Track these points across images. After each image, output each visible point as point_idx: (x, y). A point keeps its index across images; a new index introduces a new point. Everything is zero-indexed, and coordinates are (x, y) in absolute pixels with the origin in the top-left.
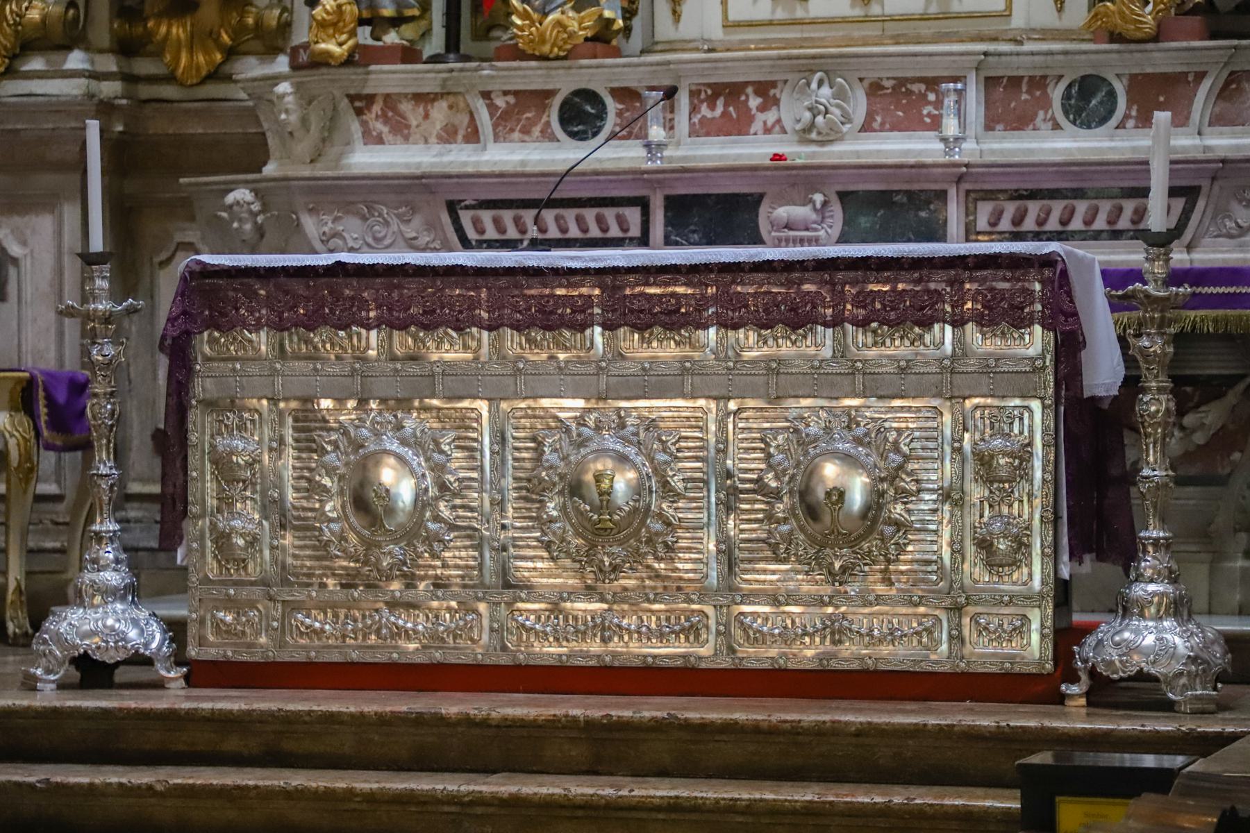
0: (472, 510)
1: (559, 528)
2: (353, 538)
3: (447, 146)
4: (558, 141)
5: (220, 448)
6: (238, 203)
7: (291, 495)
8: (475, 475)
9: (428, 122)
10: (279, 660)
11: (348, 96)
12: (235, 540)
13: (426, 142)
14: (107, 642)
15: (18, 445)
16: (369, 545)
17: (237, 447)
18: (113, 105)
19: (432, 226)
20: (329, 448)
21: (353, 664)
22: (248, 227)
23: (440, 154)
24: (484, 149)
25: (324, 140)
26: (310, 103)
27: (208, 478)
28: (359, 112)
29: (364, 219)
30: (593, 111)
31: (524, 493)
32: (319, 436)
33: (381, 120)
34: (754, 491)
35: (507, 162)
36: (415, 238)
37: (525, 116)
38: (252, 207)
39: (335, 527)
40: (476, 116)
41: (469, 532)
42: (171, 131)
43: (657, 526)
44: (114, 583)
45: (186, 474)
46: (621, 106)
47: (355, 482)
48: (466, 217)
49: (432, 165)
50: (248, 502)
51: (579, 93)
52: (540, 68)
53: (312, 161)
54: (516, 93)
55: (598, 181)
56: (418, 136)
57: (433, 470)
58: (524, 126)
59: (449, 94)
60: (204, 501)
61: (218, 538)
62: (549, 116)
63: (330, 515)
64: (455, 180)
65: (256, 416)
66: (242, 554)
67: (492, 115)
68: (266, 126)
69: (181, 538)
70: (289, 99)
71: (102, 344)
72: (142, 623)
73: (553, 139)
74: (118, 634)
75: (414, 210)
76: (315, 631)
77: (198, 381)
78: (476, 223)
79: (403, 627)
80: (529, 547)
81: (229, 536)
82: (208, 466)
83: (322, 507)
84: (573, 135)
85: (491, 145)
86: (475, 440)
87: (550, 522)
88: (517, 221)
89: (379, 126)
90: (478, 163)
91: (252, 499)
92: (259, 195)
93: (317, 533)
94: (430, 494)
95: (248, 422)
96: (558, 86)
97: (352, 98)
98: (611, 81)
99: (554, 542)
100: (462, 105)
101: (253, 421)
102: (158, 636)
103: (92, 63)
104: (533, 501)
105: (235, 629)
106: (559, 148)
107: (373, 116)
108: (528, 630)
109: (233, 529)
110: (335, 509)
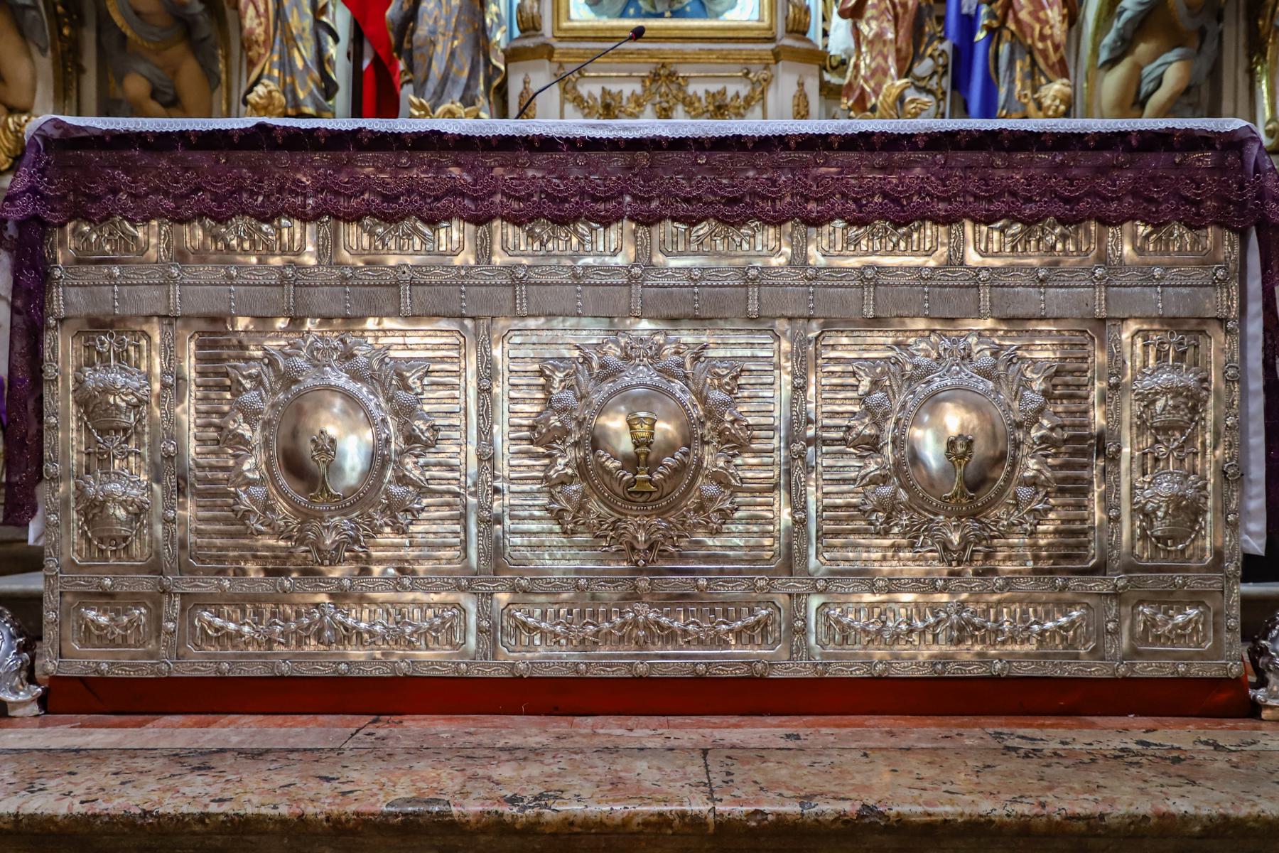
0: (451, 468)
1: (576, 492)
2: (282, 506)
5: (90, 384)
7: (192, 448)
10: (175, 674)
16: (307, 516)
17: (114, 383)
20: (248, 384)
21: (282, 678)
31: (525, 446)
32: (234, 367)
34: (844, 441)
39: (257, 491)
43: (712, 489)
47: (285, 430)
50: (132, 459)
57: (397, 414)
61: (87, 507)
63: (250, 475)
66: (124, 531)
69: (34, 511)
76: (229, 635)
77: (57, 294)
79: (354, 628)
80: (532, 518)
81: (103, 505)
82: (73, 409)
83: (239, 465)
87: (563, 483)
93: (231, 501)
94: (393, 446)
95: (132, 349)
99: (567, 511)
104: (538, 456)
105: (113, 633)
108: (531, 630)
109: (109, 496)
110: (256, 468)
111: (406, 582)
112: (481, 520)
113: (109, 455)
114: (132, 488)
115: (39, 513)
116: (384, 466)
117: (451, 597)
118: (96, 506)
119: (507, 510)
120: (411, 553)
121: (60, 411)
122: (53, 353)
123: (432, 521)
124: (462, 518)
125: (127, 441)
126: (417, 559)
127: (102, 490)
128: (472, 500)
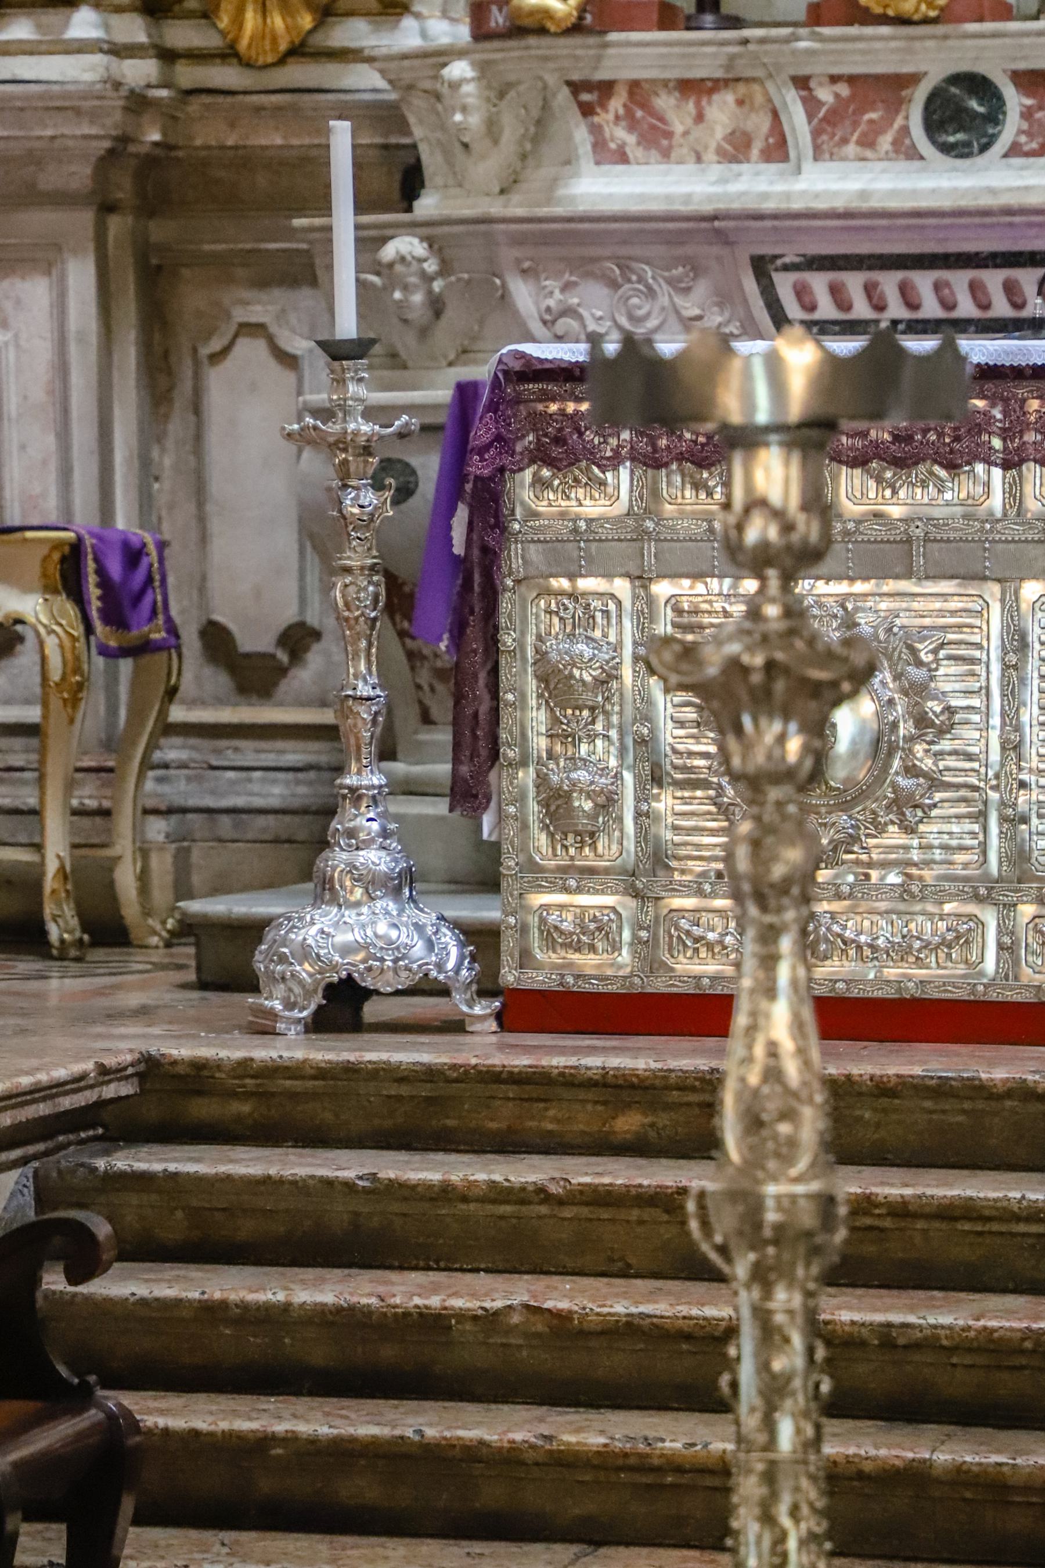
0: (970, 757)
3: (735, 167)
4: (922, 158)
5: (554, 656)
6: (403, 259)
8: (975, 702)
9: (701, 126)
10: (649, 990)
11: (569, 83)
12: (576, 804)
13: (699, 159)
15: (61, 646)
18: (144, 97)
19: (725, 297)
22: (418, 298)
23: (723, 181)
24: (798, 170)
25: (524, 157)
26: (502, 95)
27: (533, 702)
28: (586, 110)
29: (614, 285)
30: (981, 110)
33: (623, 123)
35: (836, 194)
36: (699, 318)
37: (867, 117)
38: (425, 265)
40: (783, 118)
41: (963, 793)
42: (230, 142)
44: (383, 867)
46: (1029, 102)
48: (784, 284)
49: (710, 198)
51: (956, 79)
52: (893, 38)
53: (502, 192)
54: (852, 80)
55: (1011, 225)
56: (685, 151)
57: (906, 693)
58: (864, 134)
59: (738, 80)
61: (549, 798)
62: (907, 118)
64: (768, 223)
65: (612, 607)
67: (810, 116)
68: (418, 132)
70: (468, 88)
71: (357, 488)
72: (430, 930)
73: (913, 154)
75: (697, 269)
76: (710, 946)
77: (516, 549)
78: (802, 293)
79: (853, 941)
81: (568, 795)
84: (946, 149)
85: (808, 165)
86: (978, 646)
88: (870, 289)
89: (621, 135)
90: (788, 196)
91: (606, 737)
92: (436, 247)
93: (712, 793)
94: (902, 732)
95: (599, 615)
96: (923, 68)
97: (576, 87)
98: (1014, 59)
100: (759, 99)
101: (606, 613)
102: (454, 952)
103: (107, 27)
106: (924, 170)
107: (611, 116)
111: (915, 889)
112: (1003, 819)
114: (601, 776)
116: (890, 755)
117: (971, 908)
118: (560, 796)
119: (1035, 808)
120: (915, 856)
123: (947, 819)
124: (981, 817)
125: (593, 722)
126: (928, 863)
127: (568, 778)
128: (994, 796)
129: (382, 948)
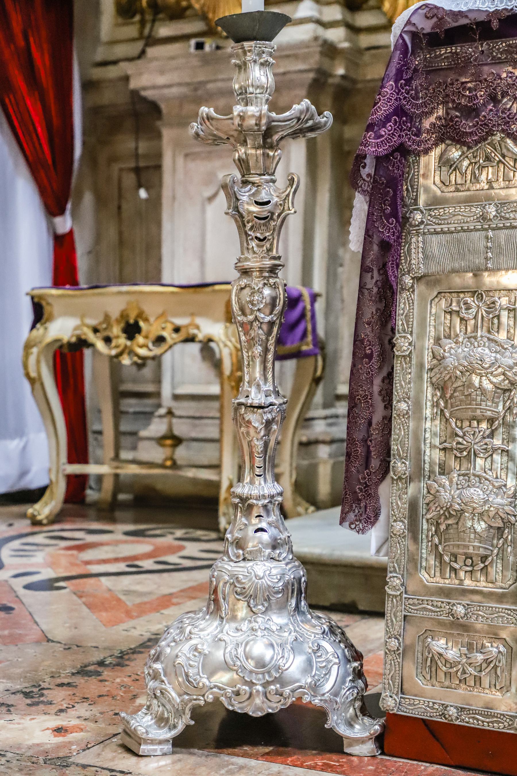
5: (450, 361)
12: (469, 524)
14: (251, 684)
27: (428, 412)
45: (389, 405)
50: (497, 457)
60: (419, 453)
74: (269, 672)
82: (428, 392)
113: (469, 452)
114: (497, 495)
115: (382, 518)
118: (451, 515)
121: (412, 394)
122: (407, 322)
125: (492, 435)
129: (251, 672)
